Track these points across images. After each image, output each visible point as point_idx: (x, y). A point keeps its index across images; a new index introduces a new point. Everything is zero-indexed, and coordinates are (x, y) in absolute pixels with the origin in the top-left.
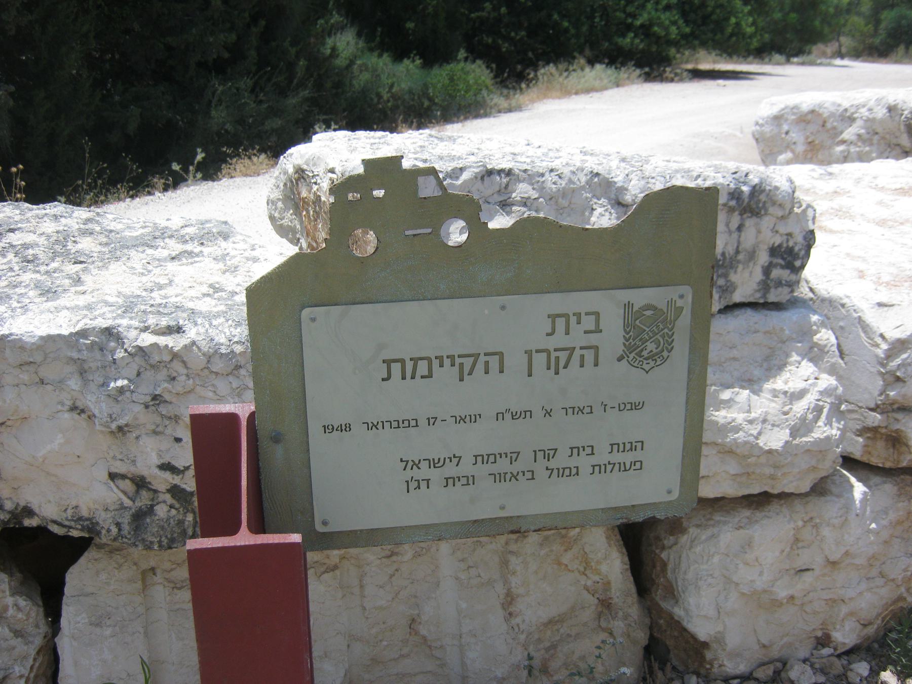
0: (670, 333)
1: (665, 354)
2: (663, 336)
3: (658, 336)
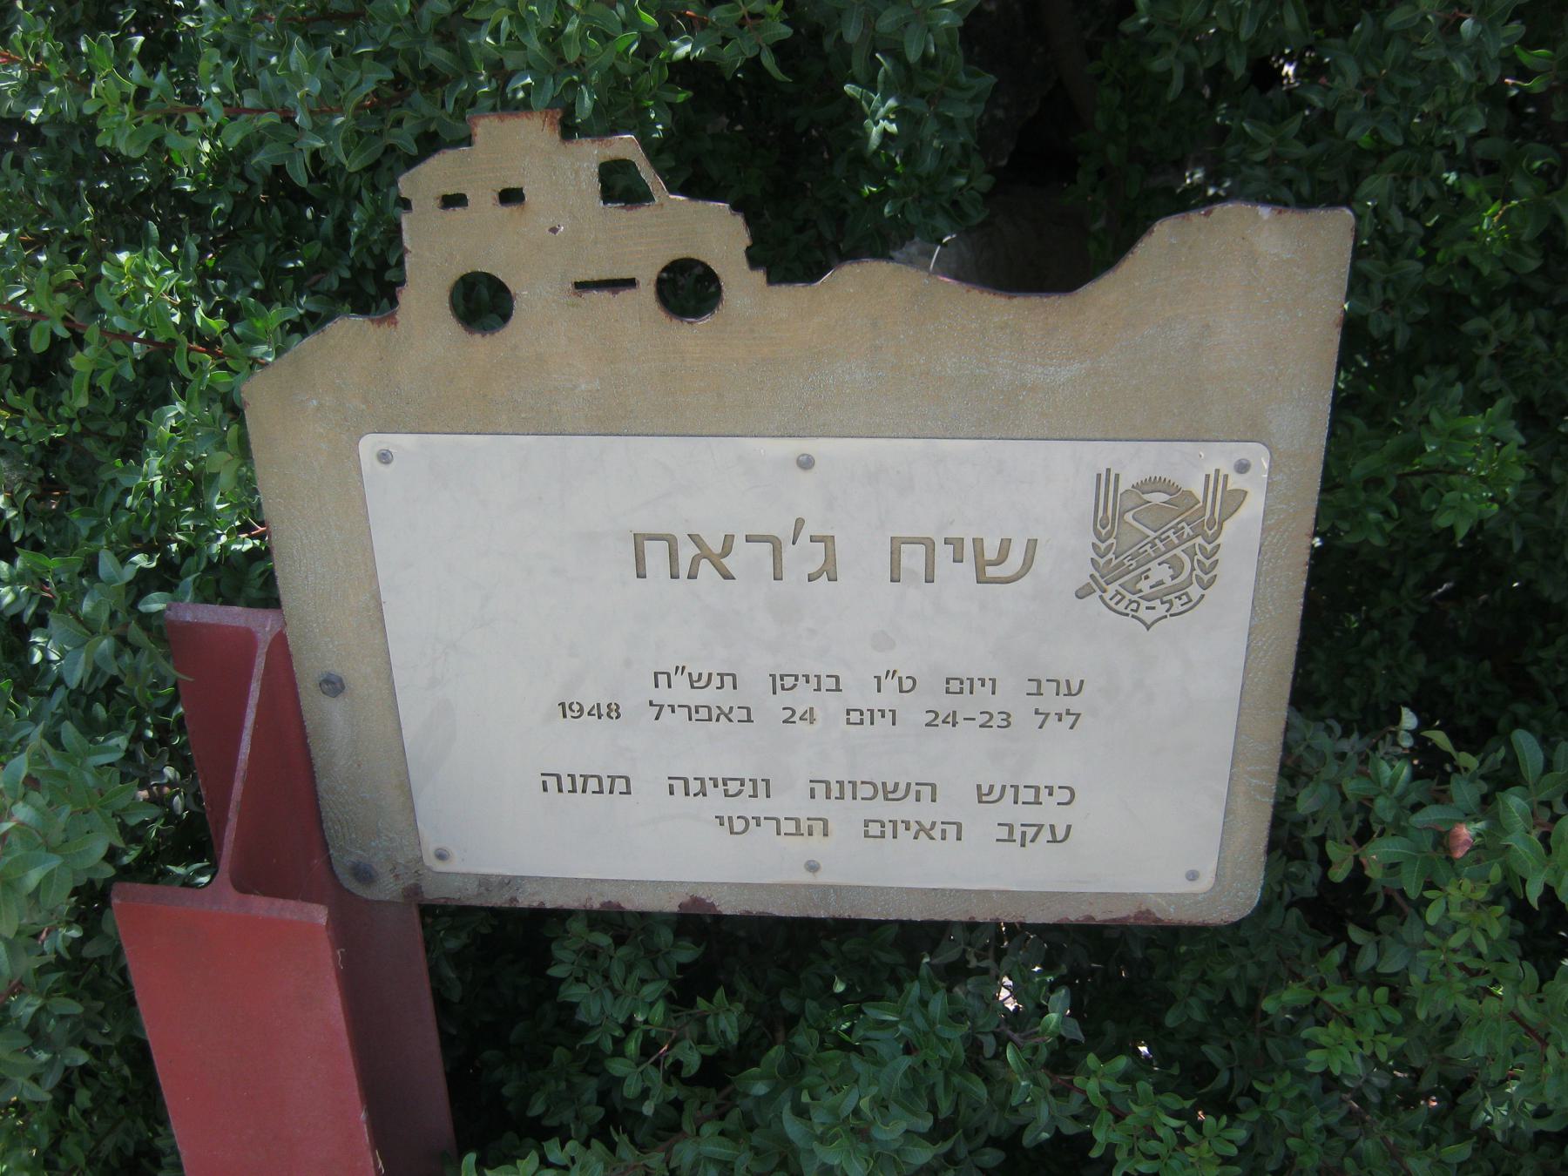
0: (1209, 547)
1: (1195, 591)
3: (1177, 551)
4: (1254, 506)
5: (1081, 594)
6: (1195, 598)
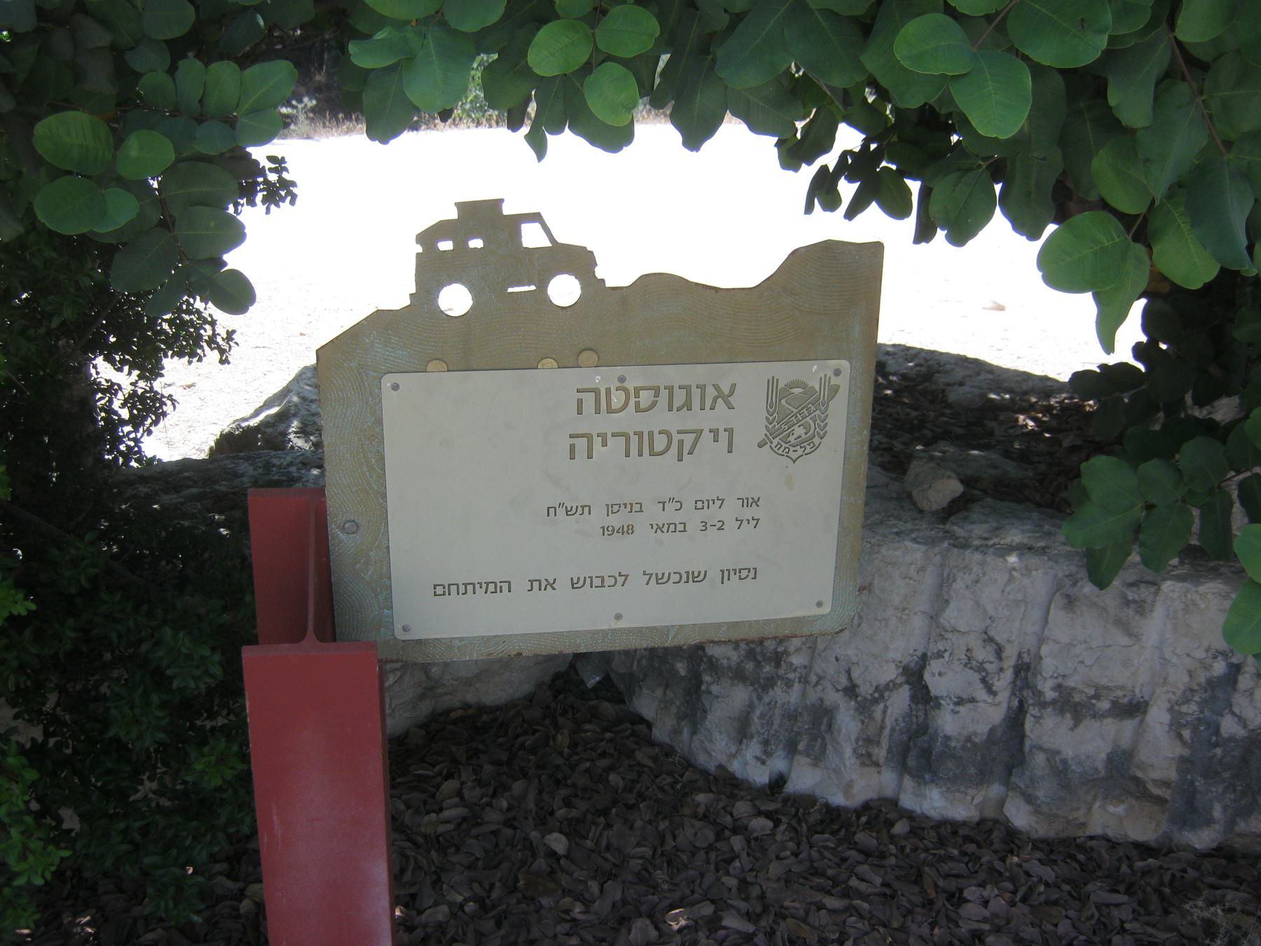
1: (816, 440)
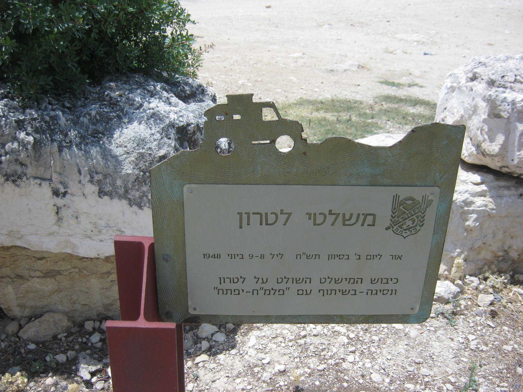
0: (423, 215)
1: (418, 228)
2: (417, 217)
3: (414, 217)
4: (435, 204)
5: (387, 229)
6: (418, 230)
